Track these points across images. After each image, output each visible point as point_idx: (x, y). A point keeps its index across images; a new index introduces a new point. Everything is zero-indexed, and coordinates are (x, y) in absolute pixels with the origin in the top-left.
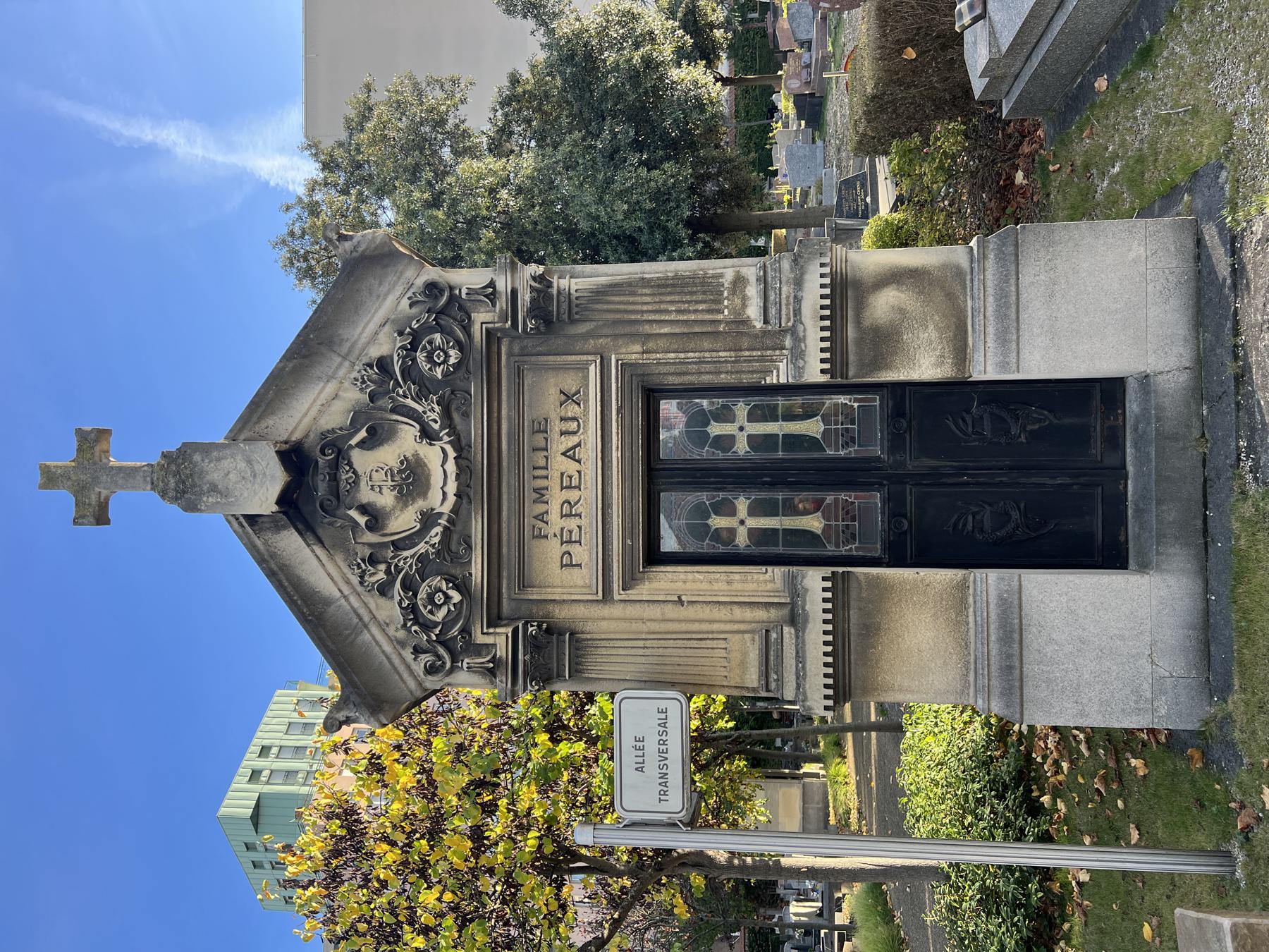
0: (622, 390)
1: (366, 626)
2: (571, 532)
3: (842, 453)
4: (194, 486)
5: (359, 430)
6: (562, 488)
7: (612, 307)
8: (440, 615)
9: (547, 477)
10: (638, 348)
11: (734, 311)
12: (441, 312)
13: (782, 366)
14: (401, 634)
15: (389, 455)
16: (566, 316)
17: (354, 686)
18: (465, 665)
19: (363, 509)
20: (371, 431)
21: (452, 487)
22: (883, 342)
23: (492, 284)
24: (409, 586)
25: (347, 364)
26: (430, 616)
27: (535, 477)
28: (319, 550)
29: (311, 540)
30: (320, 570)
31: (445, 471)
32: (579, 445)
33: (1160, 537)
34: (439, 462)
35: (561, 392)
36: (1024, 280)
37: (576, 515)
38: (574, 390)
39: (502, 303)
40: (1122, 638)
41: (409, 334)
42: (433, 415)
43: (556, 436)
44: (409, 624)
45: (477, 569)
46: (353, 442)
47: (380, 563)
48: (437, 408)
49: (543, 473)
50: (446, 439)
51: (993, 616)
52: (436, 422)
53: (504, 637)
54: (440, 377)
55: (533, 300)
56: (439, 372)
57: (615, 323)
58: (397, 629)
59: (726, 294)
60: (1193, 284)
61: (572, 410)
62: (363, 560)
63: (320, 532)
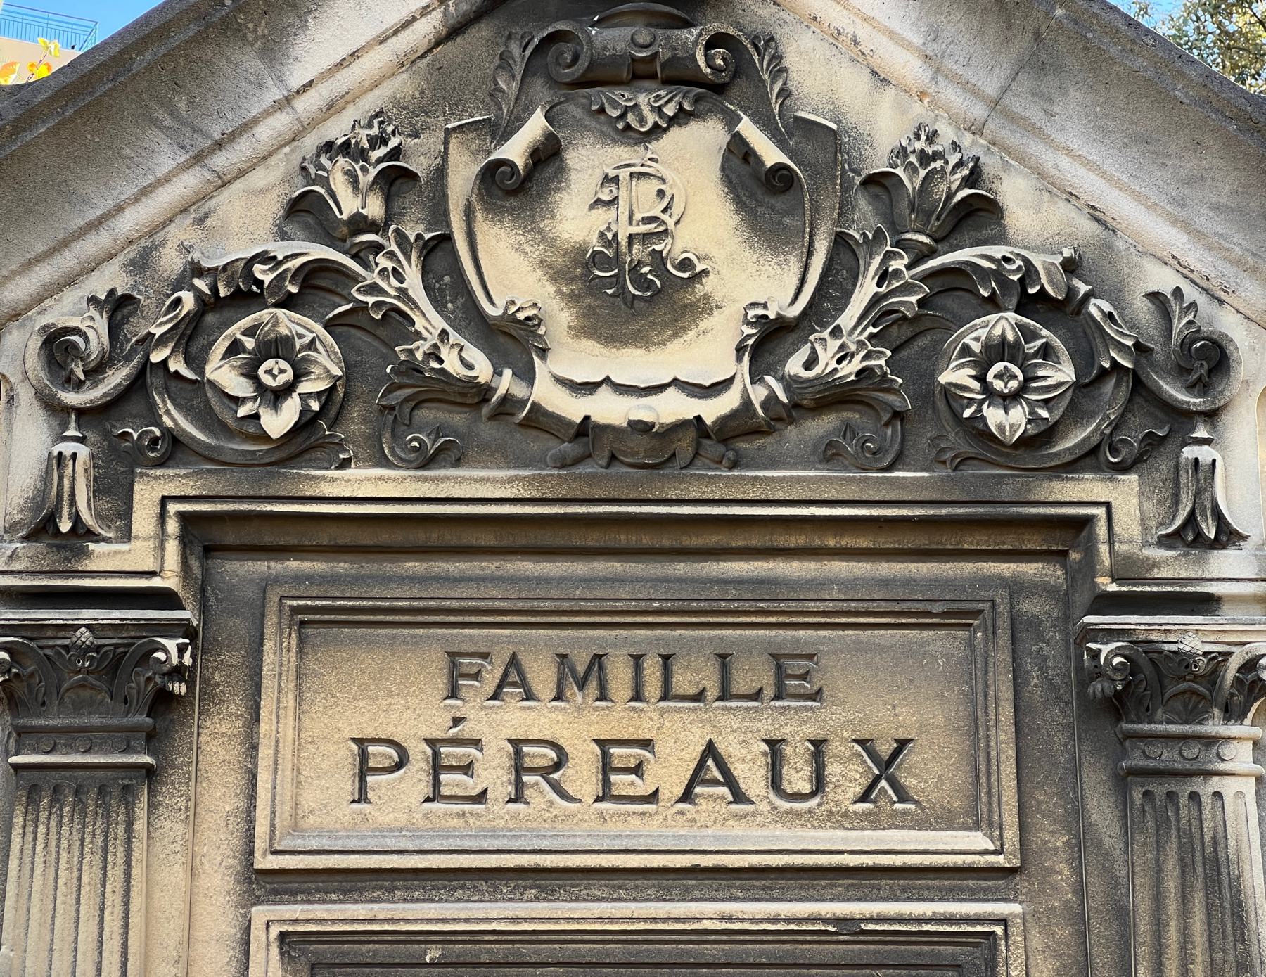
1: (198, 159)
2: (467, 769)
5: (782, 145)
7: (1172, 906)
8: (225, 375)
9: (637, 696)
12: (1139, 387)
14: (171, 261)
15: (707, 227)
16: (1137, 761)
18: (67, 448)
19: (547, 156)
20: (780, 180)
21: (609, 410)
23: (1228, 536)
24: (315, 284)
25: (979, 111)
26: (221, 346)
27: (637, 659)
31: (659, 389)
32: (739, 796)
34: (689, 370)
35: (903, 744)
37: (519, 786)
38: (909, 782)
39: (1171, 566)
41: (1071, 291)
42: (830, 357)
44: (201, 284)
45: (359, 484)
46: (748, 129)
47: (388, 200)
48: (849, 369)
49: (653, 685)
50: (758, 395)
52: (810, 364)
53: (149, 565)
54: (945, 378)
55: (1183, 659)
56: (957, 375)
57: (1122, 916)
58: (185, 248)
61: (848, 777)
62: (396, 153)
63: (482, 32)
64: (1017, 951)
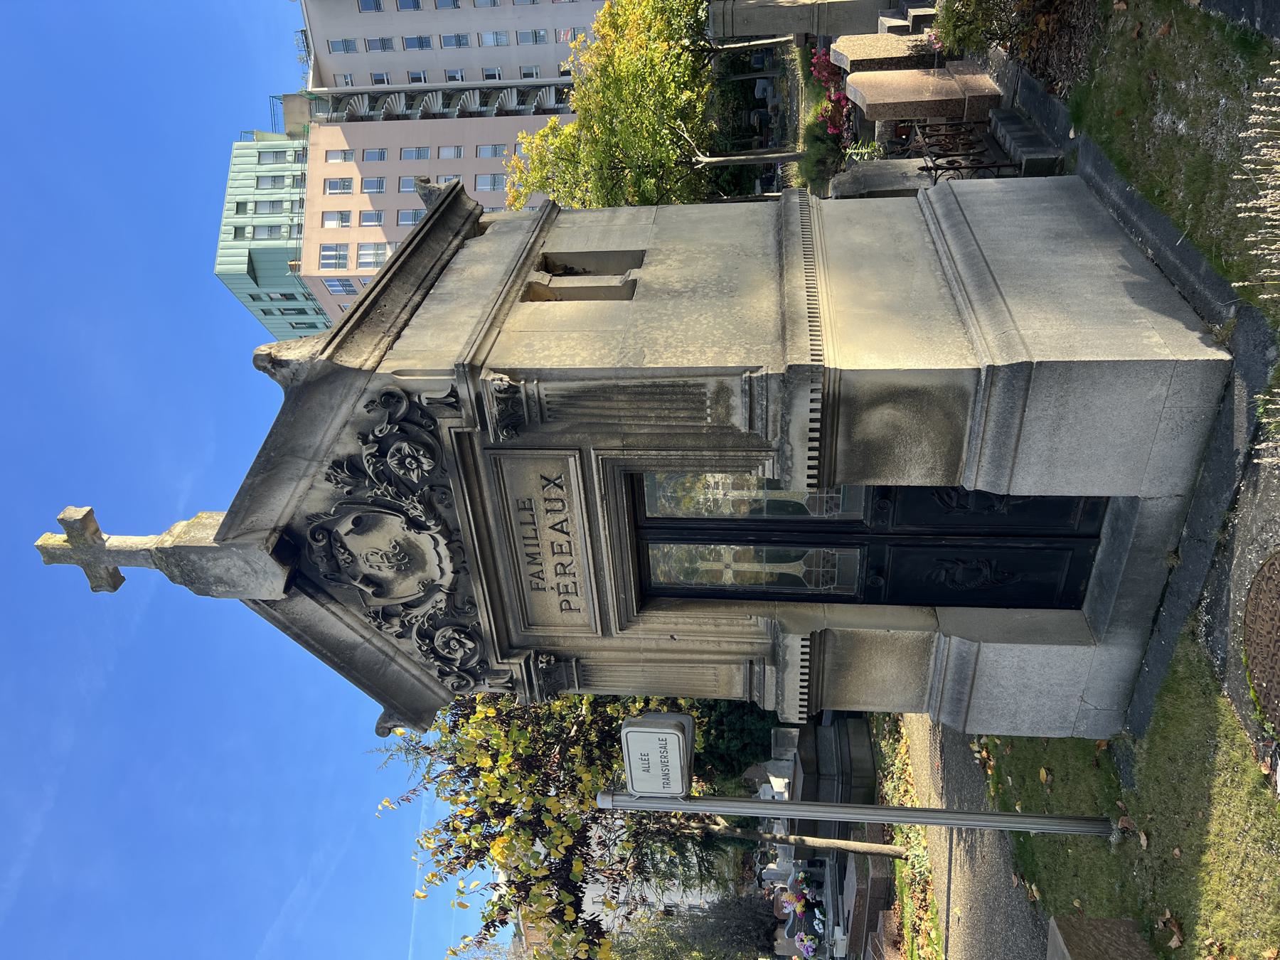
0: (605, 480)
1: (392, 659)
3: (826, 516)
4: (200, 578)
6: (554, 554)
7: (587, 411)
10: (617, 442)
11: (716, 418)
13: (768, 464)
16: (538, 419)
17: (395, 708)
19: (368, 580)
20: (356, 522)
22: (873, 453)
23: (454, 393)
28: (333, 608)
29: (323, 599)
30: (340, 623)
31: (438, 553)
33: (1113, 622)
35: (542, 477)
36: (1030, 414)
38: (555, 476)
40: (1061, 685)
41: (374, 442)
42: (418, 512)
43: (542, 513)
45: (484, 620)
49: (535, 542)
51: (951, 664)
55: (501, 413)
56: (414, 477)
59: (708, 403)
60: (1209, 423)
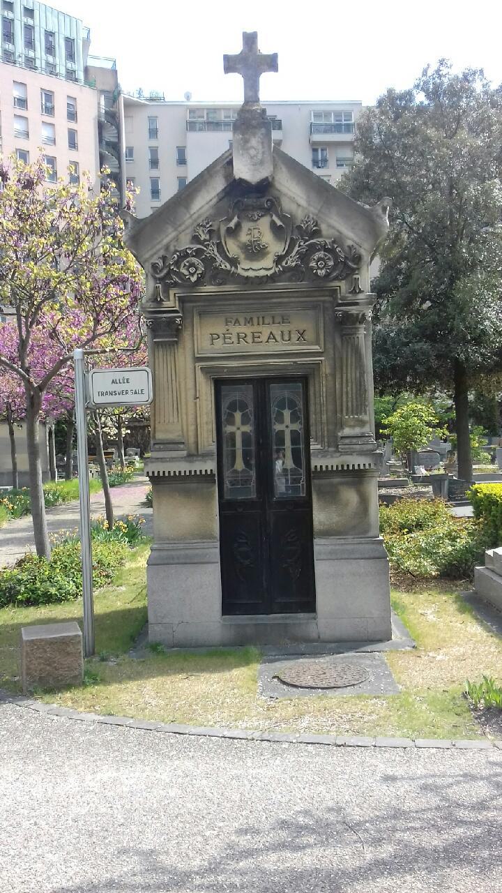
2: (230, 338)
5: (281, 221)
6: (253, 333)
8: (184, 271)
9: (258, 324)
10: (328, 371)
12: (345, 264)
13: (319, 447)
14: (172, 248)
15: (267, 238)
18: (157, 285)
19: (238, 225)
21: (251, 274)
22: (331, 496)
23: (361, 291)
24: (198, 253)
25: (317, 212)
26: (182, 265)
27: (258, 318)
28: (215, 200)
29: (221, 196)
32: (276, 341)
34: (264, 267)
37: (239, 340)
39: (350, 297)
41: (333, 247)
42: (291, 262)
44: (178, 253)
45: (209, 289)
46: (275, 218)
47: (210, 236)
48: (294, 264)
49: (261, 323)
50: (277, 269)
52: (286, 263)
53: (173, 306)
54: (311, 265)
56: (313, 264)
57: (341, 359)
58: (175, 246)
59: (356, 416)
61: (295, 336)
62: (211, 226)
63: (225, 200)
64: (324, 366)
